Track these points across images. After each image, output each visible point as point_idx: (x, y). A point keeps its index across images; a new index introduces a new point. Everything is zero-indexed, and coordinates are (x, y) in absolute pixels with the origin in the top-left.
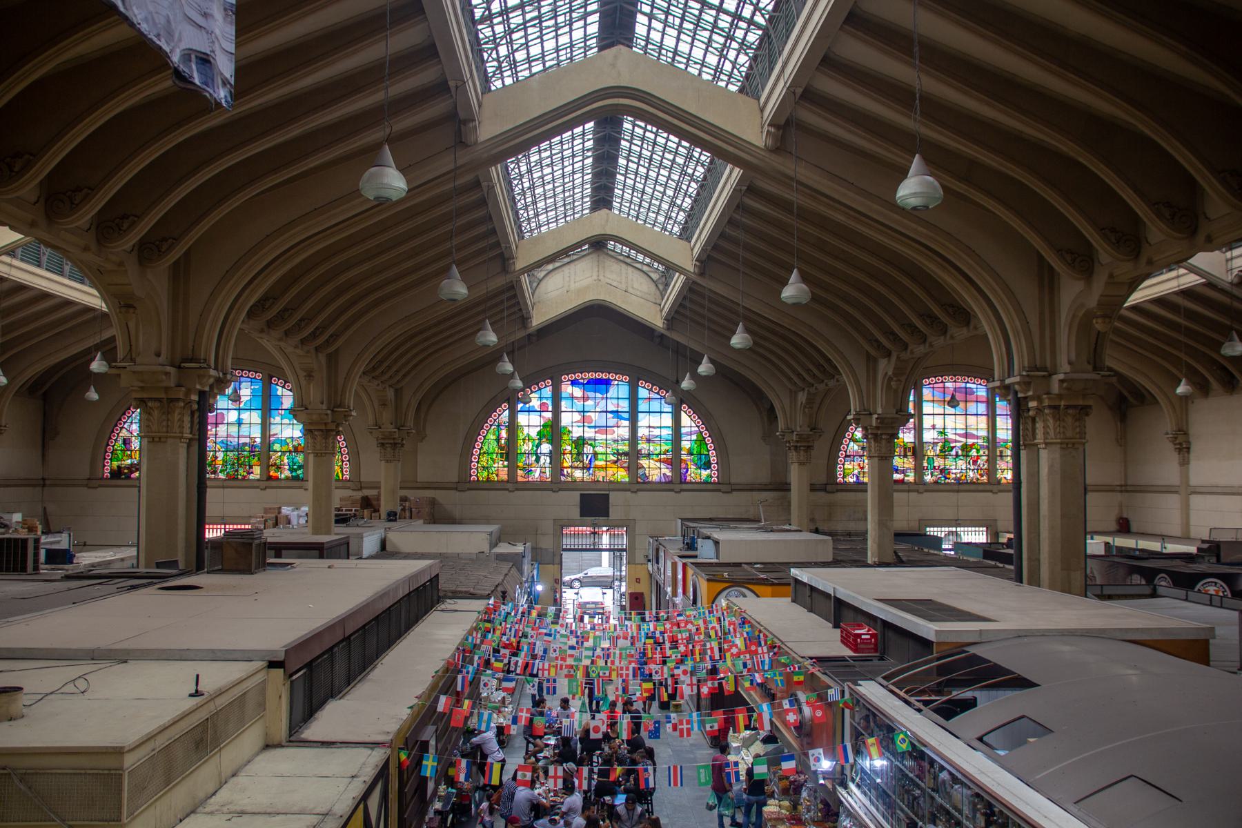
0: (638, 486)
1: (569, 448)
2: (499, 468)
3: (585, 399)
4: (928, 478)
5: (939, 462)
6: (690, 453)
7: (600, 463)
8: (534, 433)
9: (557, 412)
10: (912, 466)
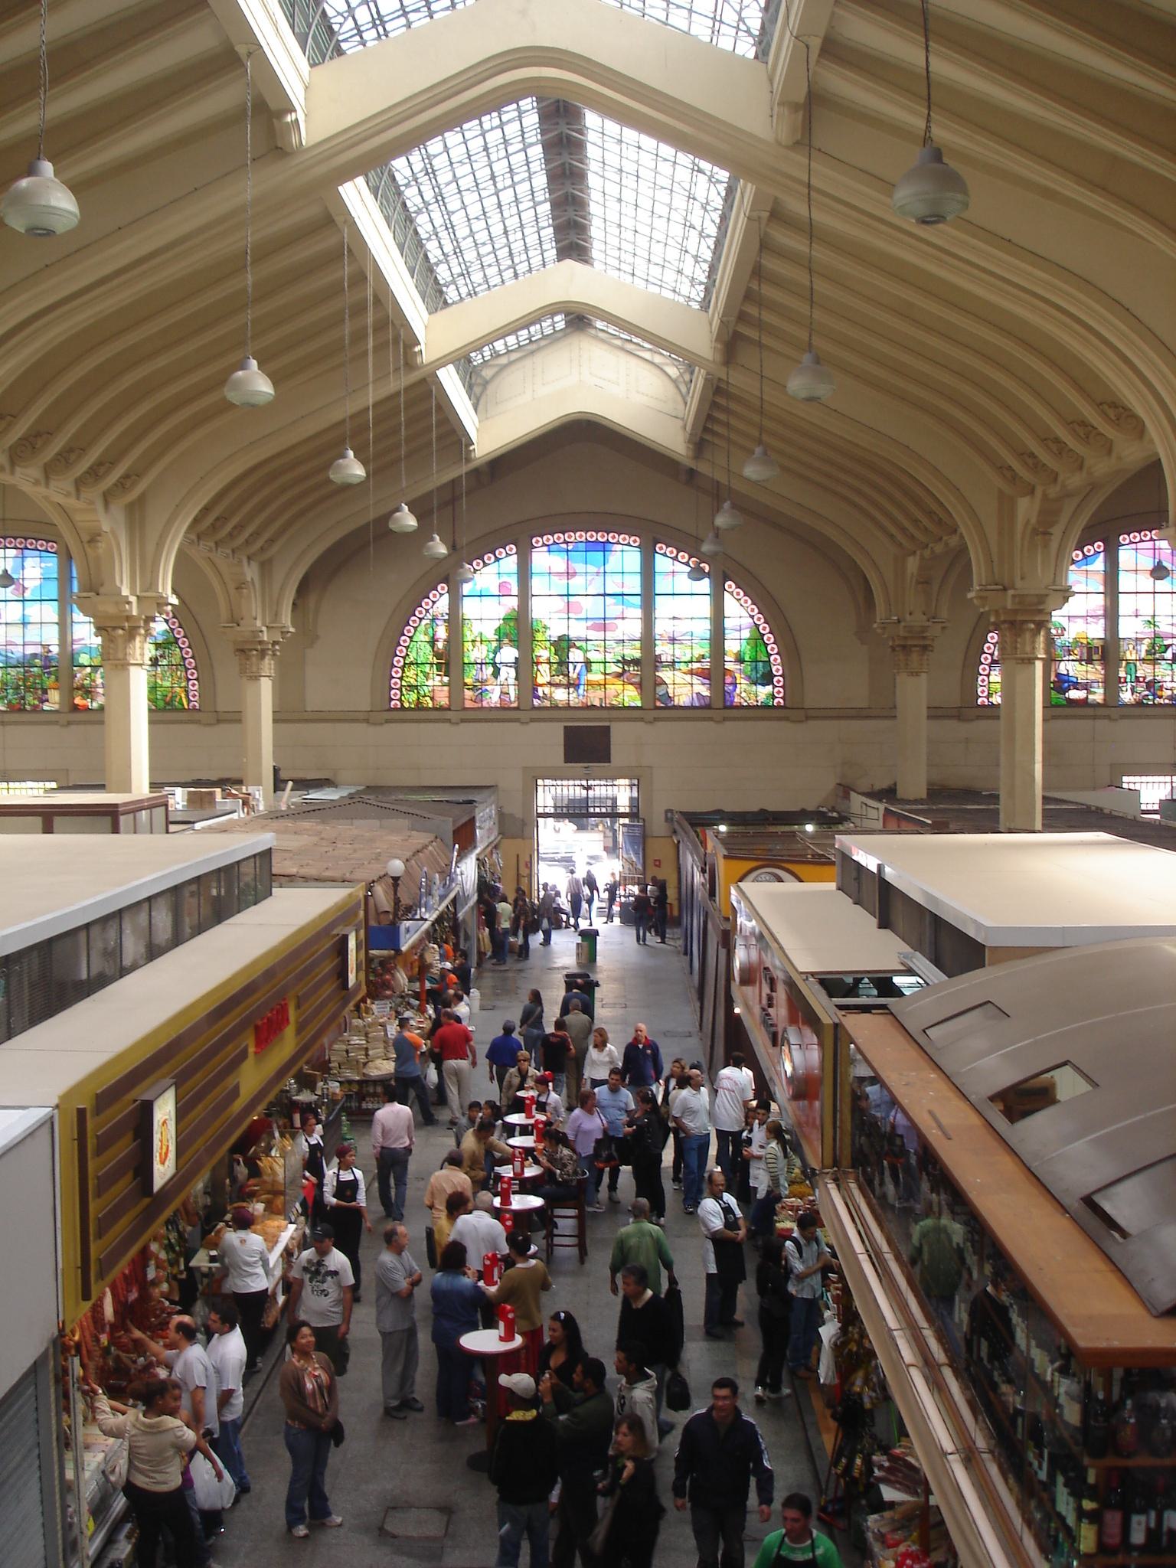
0: (657, 714)
2: (435, 686)
3: (569, 574)
4: (1127, 697)
5: (1144, 671)
6: (740, 660)
7: (596, 676)
8: (489, 630)
9: (525, 594)
10: (1100, 677)
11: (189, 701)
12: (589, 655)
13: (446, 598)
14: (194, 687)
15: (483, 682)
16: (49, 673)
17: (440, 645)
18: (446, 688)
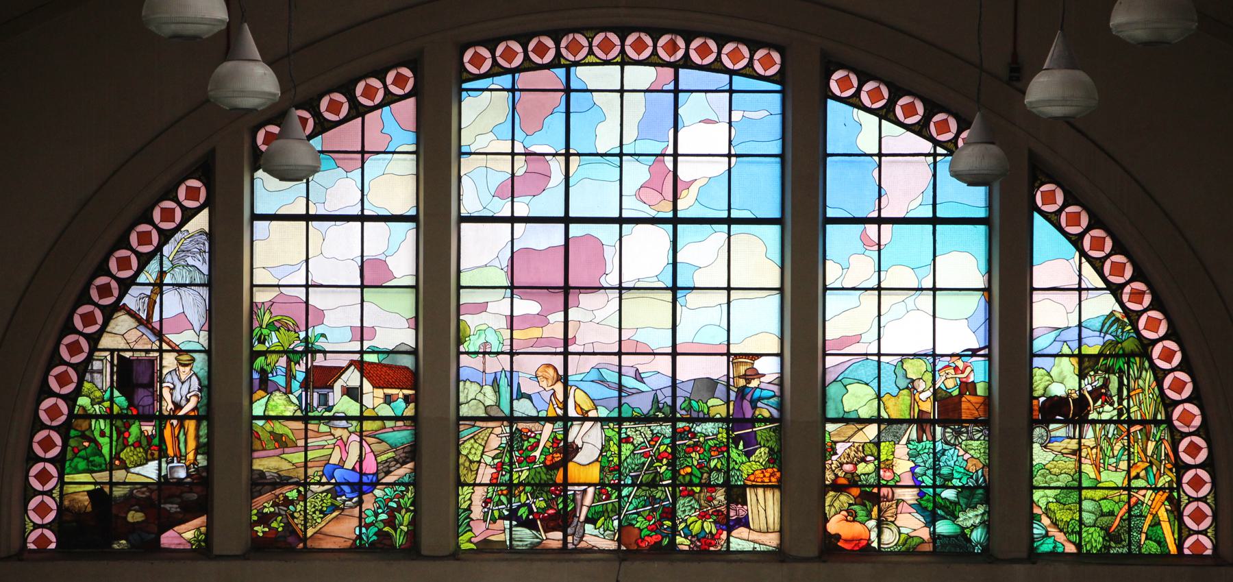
11: (1183, 533)
14: (1198, 491)
16: (750, 443)
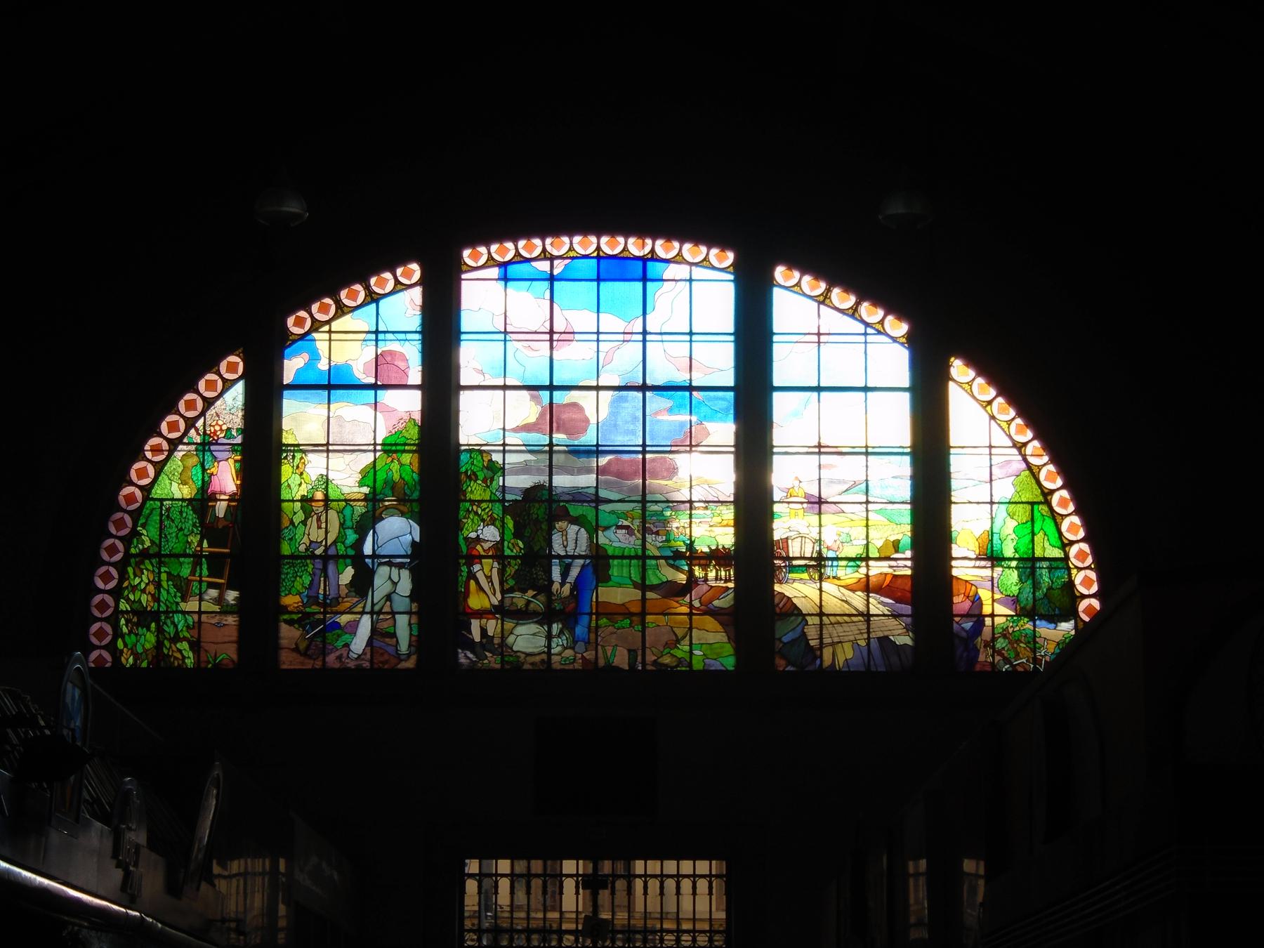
1: (491, 534)
7: (617, 593)
12: (602, 539)
13: (236, 396)
15: (331, 604)
17: (221, 508)
18: (231, 620)
